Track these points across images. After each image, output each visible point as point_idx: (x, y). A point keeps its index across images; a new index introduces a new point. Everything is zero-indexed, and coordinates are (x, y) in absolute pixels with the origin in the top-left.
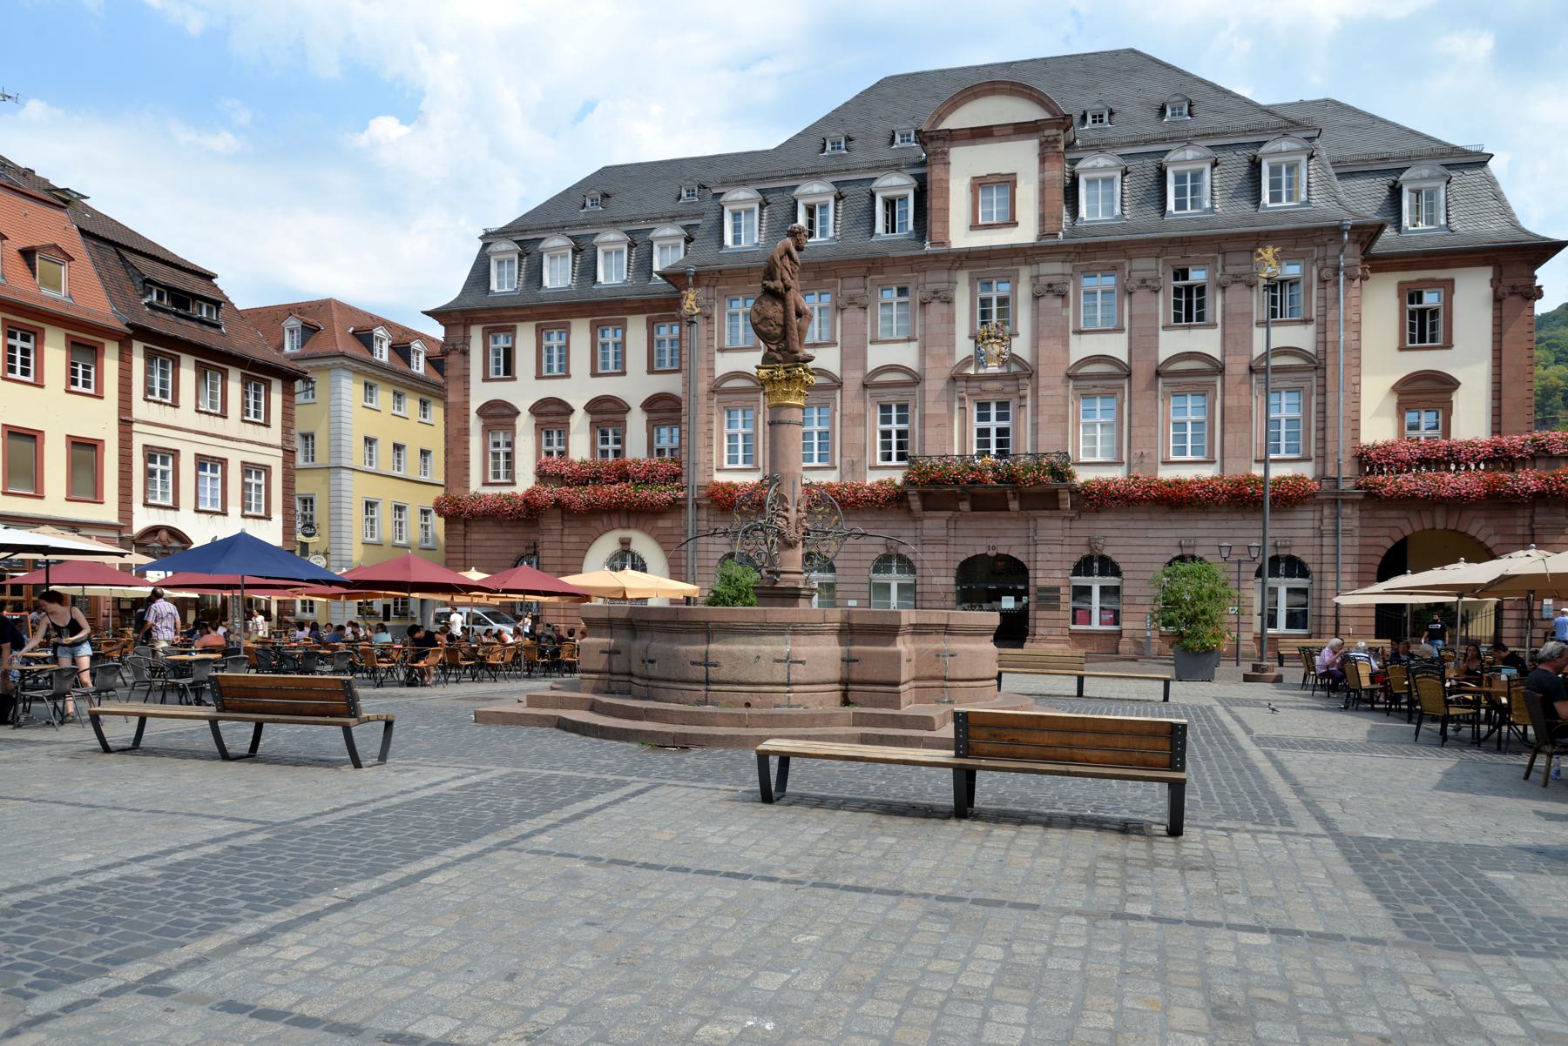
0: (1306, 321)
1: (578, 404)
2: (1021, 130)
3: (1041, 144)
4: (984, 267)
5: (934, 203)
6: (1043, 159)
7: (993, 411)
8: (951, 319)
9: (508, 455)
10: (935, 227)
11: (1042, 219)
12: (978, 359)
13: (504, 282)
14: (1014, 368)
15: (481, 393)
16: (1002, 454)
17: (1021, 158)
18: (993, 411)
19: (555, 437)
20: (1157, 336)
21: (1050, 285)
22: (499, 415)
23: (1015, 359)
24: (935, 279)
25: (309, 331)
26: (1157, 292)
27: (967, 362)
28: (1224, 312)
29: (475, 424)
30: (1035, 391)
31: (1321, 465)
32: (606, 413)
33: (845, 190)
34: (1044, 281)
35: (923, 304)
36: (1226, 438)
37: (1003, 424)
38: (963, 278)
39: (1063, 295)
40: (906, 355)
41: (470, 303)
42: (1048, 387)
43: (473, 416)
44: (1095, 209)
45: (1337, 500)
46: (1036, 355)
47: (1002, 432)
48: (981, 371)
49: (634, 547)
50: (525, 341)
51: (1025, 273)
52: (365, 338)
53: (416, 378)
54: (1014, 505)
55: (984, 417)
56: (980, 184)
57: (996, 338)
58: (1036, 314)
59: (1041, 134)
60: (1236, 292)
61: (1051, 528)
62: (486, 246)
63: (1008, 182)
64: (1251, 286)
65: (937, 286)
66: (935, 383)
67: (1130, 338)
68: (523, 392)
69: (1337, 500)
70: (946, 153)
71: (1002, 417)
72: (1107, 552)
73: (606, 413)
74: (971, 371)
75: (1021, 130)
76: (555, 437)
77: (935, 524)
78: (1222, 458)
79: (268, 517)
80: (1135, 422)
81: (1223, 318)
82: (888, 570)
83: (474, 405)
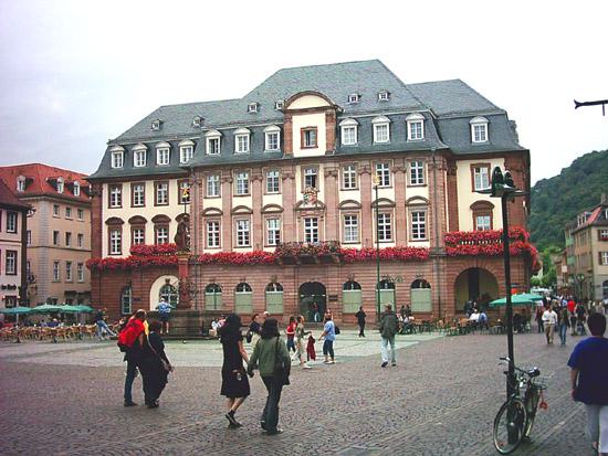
1: (149, 219)
5: (287, 138)
6: (327, 121)
7: (312, 222)
8: (294, 185)
9: (119, 241)
10: (287, 148)
12: (306, 201)
13: (116, 164)
15: (107, 214)
16: (315, 240)
17: (318, 121)
18: (312, 222)
19: (139, 233)
22: (115, 224)
24: (287, 170)
25: (29, 182)
27: (301, 202)
29: (105, 229)
32: (160, 222)
33: (255, 131)
35: (284, 179)
38: (298, 168)
39: (336, 176)
41: (103, 174)
43: (104, 224)
44: (349, 139)
45: (438, 257)
46: (326, 200)
47: (315, 231)
49: (171, 283)
50: (126, 190)
51: (322, 166)
52: (53, 183)
53: (75, 200)
54: (317, 262)
55: (308, 225)
58: (325, 184)
60: (399, 174)
61: (334, 271)
62: (110, 147)
66: (289, 212)
68: (126, 212)
69: (438, 257)
72: (355, 280)
73: (160, 222)
74: (302, 206)
76: (139, 233)
77: (289, 271)
79: (16, 274)
83: (104, 219)
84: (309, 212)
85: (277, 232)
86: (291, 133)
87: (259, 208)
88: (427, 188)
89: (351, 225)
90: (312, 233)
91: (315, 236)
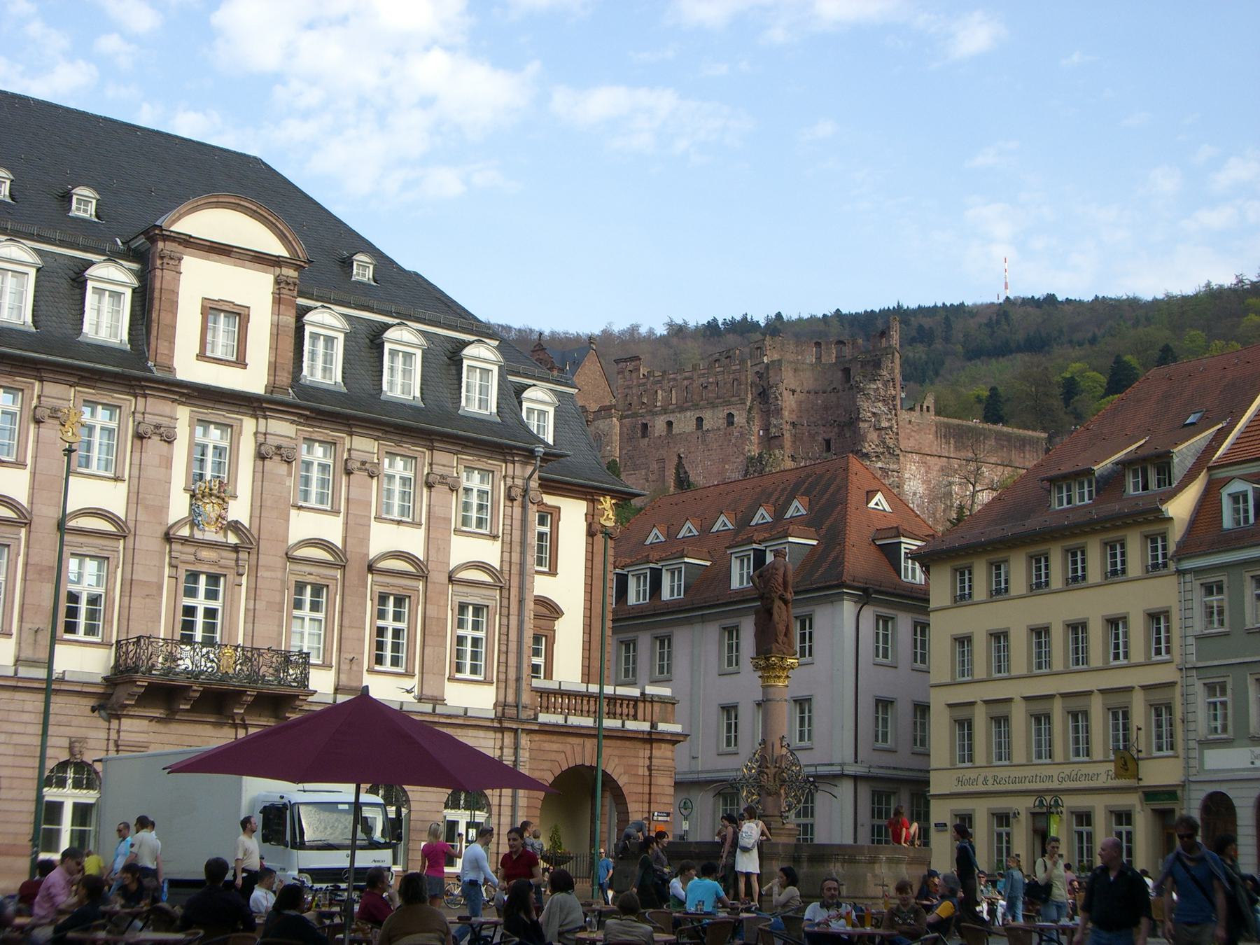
0: (495, 537)
2: (260, 259)
3: (277, 282)
4: (208, 408)
6: (278, 301)
8: (168, 463)
11: (274, 368)
12: (193, 521)
14: (232, 539)
16: (209, 642)
20: (369, 526)
21: (279, 448)
23: (235, 527)
24: (156, 408)
26: (372, 477)
28: (429, 512)
30: (255, 570)
31: (502, 691)
34: (271, 440)
36: (426, 652)
37: (212, 604)
40: (114, 498)
42: (268, 568)
47: (210, 613)
48: (198, 535)
51: (249, 425)
55: (191, 592)
56: (211, 309)
57: (218, 497)
58: (260, 477)
59: (278, 270)
63: (240, 315)
64: (453, 491)
65: (158, 420)
66: (149, 541)
67: (346, 524)
70: (180, 259)
71: (211, 595)
74: (185, 532)
75: (260, 259)
77: (135, 728)
78: (422, 673)
80: (346, 622)
81: (429, 518)
82: (61, 783)
84: (205, 554)
85: (93, 600)
86: (174, 305)
87: (55, 514)
88: (498, 544)
89: (306, 612)
90: (200, 619)
91: (210, 628)
